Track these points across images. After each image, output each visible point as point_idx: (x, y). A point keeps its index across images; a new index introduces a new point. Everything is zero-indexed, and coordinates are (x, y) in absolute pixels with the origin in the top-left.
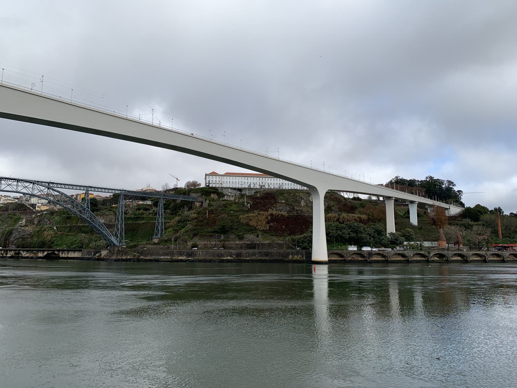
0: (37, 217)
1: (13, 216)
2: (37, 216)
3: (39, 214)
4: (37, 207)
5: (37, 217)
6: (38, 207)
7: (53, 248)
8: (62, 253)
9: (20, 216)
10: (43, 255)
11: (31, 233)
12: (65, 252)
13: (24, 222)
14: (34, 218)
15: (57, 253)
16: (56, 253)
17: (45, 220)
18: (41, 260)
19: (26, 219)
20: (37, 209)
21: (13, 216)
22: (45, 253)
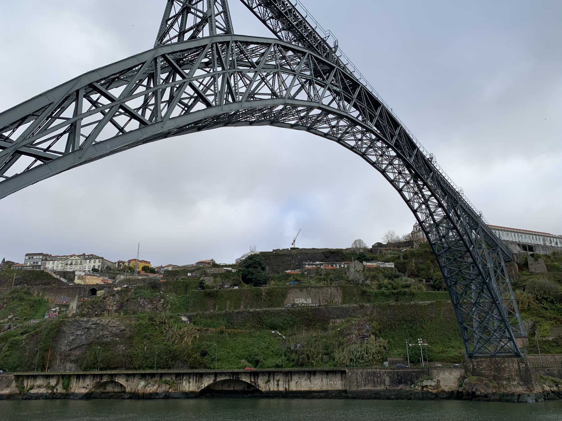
0: (114, 295)
1: (25, 296)
2: (114, 293)
3: (119, 289)
4: (76, 277)
5: (114, 295)
6: (79, 278)
7: (211, 368)
8: (269, 381)
9: (43, 296)
10: (199, 387)
11: (124, 330)
12: (277, 378)
13: (75, 307)
14: (104, 298)
15: (248, 381)
16: (246, 379)
17: (140, 302)
18: (192, 402)
19: (79, 301)
20: (77, 281)
21: (25, 296)
22: (207, 382)
